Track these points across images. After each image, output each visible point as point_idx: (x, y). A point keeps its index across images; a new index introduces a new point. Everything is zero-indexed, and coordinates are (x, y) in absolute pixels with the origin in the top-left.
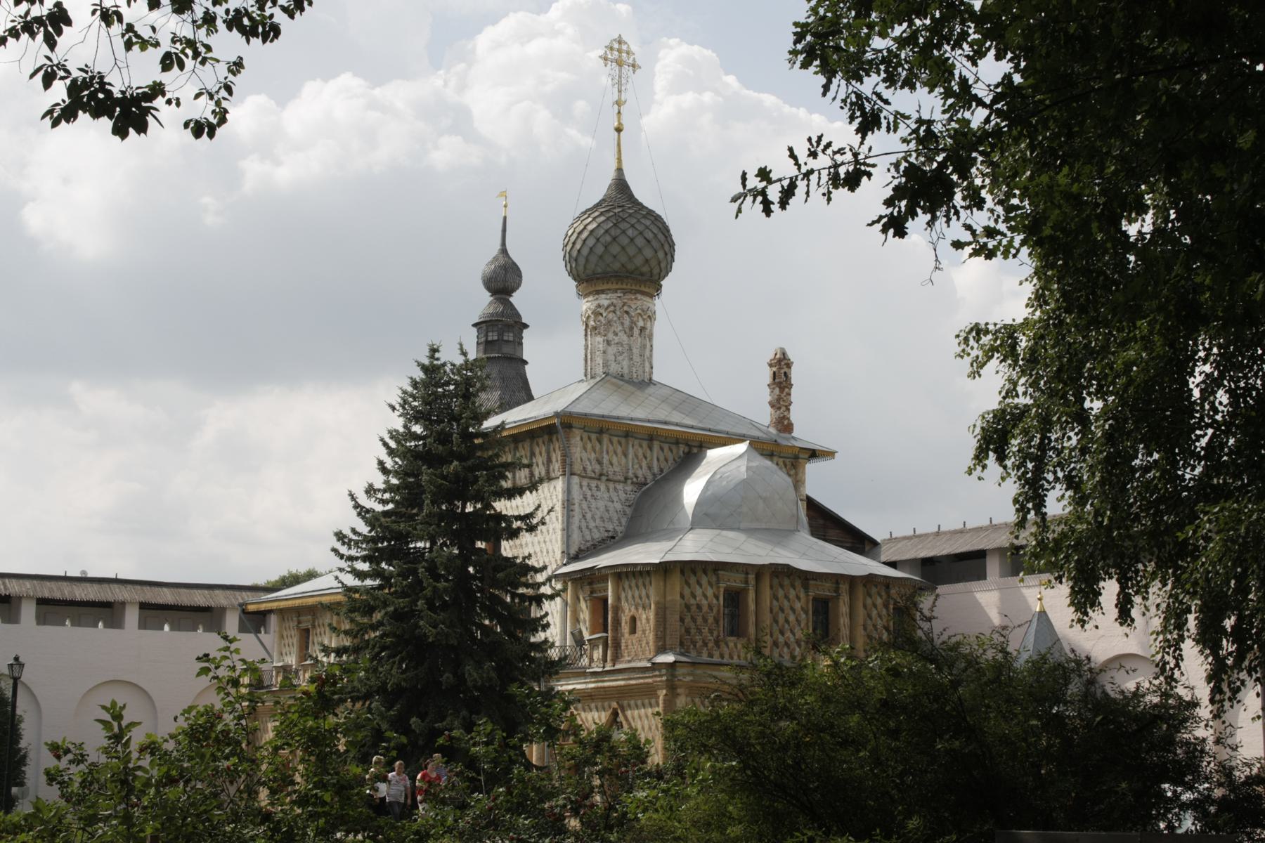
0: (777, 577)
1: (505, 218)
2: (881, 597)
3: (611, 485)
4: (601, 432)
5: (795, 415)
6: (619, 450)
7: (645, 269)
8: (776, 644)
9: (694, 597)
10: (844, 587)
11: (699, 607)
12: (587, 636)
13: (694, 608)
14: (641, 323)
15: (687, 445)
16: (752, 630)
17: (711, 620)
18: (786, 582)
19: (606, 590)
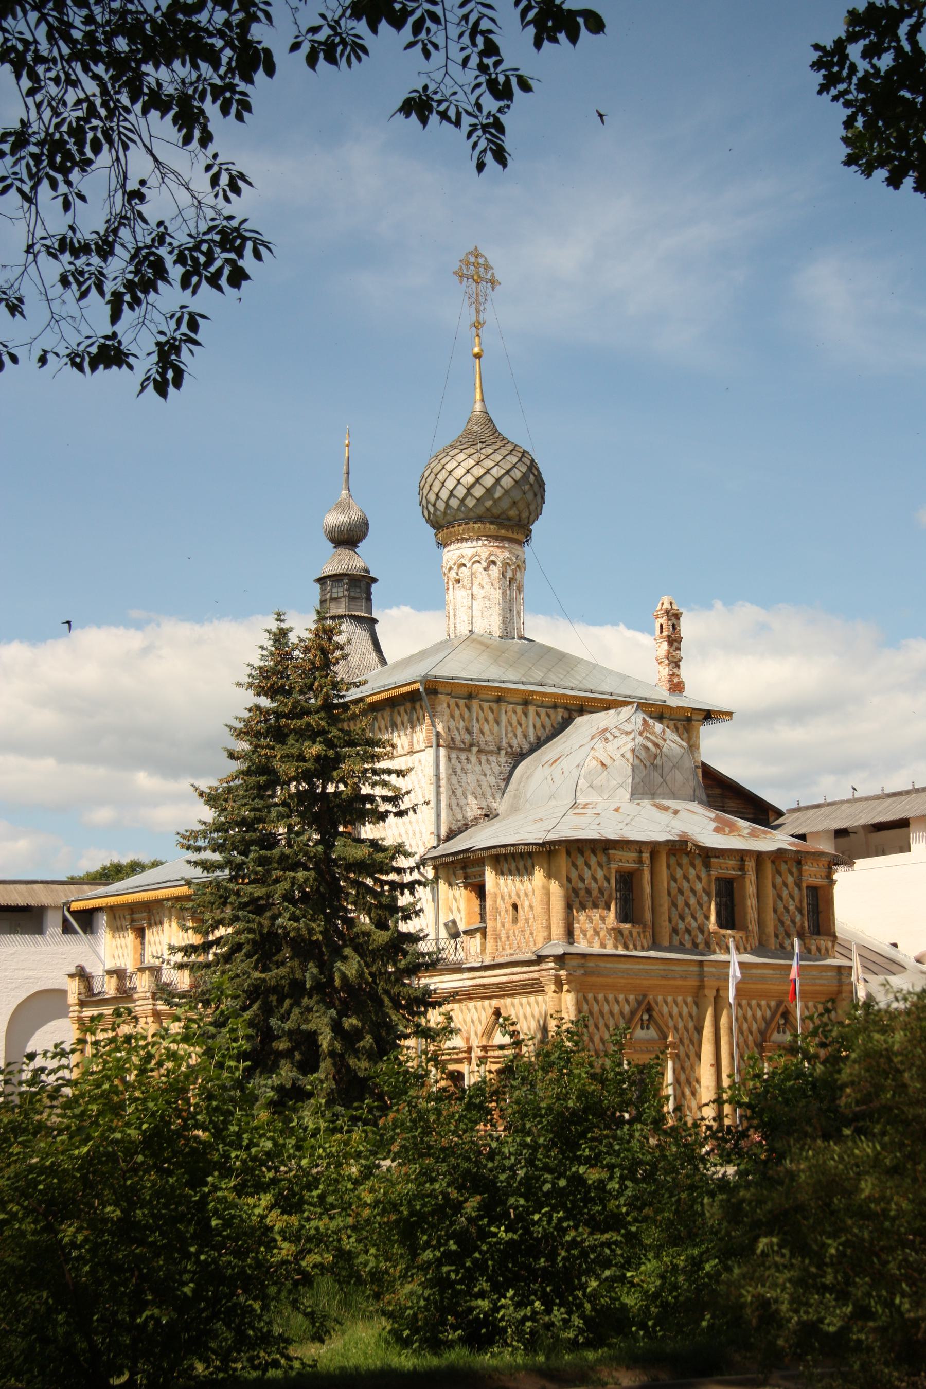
0: (675, 855)
2: (792, 874)
3: (483, 758)
4: (470, 697)
5: (686, 673)
6: (491, 717)
7: (513, 513)
8: (675, 931)
9: (582, 879)
10: (750, 864)
11: (588, 891)
12: (462, 927)
13: (582, 893)
15: (566, 709)
16: (648, 916)
18: (685, 860)
19: (483, 874)
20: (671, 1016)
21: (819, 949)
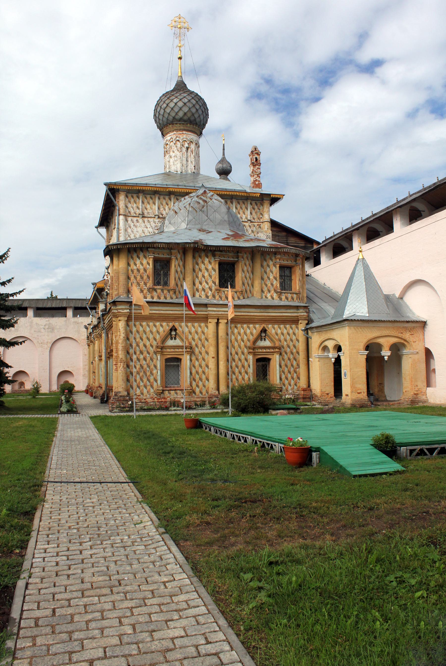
0: (198, 252)
1: (224, 144)
2: (272, 260)
3: (146, 220)
5: (263, 180)
8: (197, 290)
11: (138, 270)
13: (135, 271)
14: (186, 145)
17: (145, 277)
18: (203, 254)
20: (190, 333)
21: (287, 298)
